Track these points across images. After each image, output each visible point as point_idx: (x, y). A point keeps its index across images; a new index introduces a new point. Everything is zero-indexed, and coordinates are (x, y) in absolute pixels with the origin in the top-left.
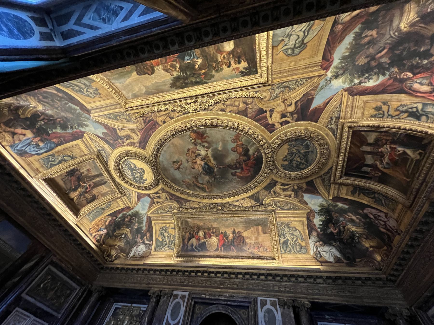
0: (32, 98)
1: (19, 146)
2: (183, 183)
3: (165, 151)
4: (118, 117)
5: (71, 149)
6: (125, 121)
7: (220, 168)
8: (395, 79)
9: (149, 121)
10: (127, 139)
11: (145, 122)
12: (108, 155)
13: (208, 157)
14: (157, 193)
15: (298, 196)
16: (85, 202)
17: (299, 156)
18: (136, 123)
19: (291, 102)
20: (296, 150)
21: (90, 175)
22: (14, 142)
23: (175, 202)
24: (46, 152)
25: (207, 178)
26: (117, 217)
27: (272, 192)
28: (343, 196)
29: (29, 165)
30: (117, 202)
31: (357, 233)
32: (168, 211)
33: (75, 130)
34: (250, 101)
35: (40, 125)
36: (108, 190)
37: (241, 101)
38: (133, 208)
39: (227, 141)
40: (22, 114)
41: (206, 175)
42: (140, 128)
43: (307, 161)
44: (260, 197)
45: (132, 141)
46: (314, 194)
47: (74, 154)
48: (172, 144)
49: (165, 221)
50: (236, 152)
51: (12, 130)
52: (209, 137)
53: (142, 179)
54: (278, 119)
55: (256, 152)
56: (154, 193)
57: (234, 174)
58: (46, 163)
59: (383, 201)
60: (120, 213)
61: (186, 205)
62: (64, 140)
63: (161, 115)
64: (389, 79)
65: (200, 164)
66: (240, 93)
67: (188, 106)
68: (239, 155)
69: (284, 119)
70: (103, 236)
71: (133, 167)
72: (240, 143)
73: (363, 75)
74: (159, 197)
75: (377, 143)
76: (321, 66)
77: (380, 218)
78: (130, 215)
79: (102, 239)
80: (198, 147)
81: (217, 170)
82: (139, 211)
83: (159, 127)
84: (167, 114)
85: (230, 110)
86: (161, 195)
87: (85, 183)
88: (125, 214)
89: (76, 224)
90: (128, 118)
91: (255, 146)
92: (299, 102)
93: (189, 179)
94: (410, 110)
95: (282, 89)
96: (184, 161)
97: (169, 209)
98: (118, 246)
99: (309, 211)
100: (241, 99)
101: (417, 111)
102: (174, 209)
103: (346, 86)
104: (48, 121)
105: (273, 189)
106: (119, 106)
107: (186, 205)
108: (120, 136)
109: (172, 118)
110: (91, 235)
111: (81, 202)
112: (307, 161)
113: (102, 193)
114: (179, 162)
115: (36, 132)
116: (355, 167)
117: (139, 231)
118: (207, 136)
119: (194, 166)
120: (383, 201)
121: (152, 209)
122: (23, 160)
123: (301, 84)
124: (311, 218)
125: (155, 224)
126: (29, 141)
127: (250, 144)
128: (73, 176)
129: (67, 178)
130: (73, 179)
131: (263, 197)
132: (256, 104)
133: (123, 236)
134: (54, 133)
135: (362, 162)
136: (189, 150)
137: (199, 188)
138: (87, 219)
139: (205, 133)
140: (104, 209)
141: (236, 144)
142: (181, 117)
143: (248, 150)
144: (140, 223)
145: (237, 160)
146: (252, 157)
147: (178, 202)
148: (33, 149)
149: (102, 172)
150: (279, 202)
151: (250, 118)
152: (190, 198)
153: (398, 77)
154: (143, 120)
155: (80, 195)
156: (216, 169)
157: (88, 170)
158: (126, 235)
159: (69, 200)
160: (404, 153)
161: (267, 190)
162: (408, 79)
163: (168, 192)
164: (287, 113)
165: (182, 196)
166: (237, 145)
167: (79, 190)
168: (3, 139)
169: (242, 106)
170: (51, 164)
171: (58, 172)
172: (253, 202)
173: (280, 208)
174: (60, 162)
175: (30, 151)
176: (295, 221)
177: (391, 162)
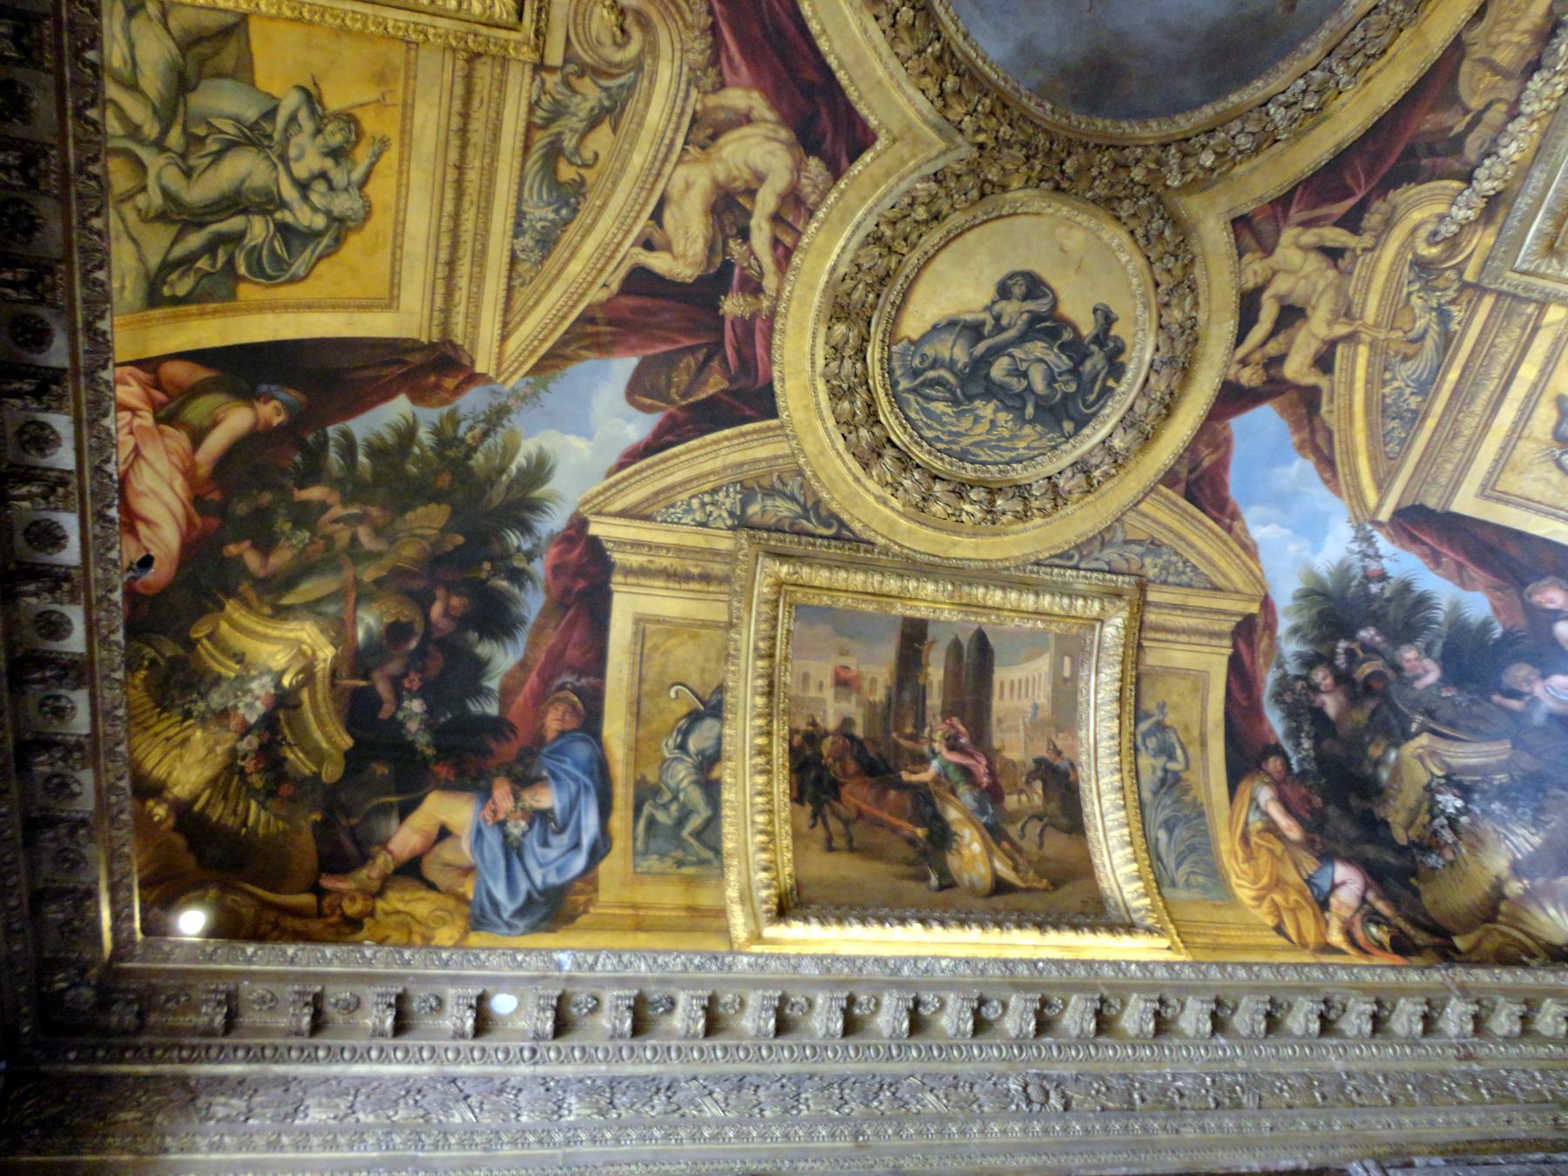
0: (231, 606)
1: (500, 893)
4: (566, 172)
5: (651, 672)
6: (604, 130)
10: (744, 234)
12: (793, 486)
16: (1057, 844)
18: (656, 58)
21: (880, 696)
22: (461, 899)
24: (605, 810)
26: (1277, 750)
30: (1167, 672)
32: (1443, 316)
33: (539, 568)
35: (428, 725)
36: (1043, 664)
38: (1267, 604)
40: (319, 764)
42: (699, 47)
45: (766, 201)
47: (694, 680)
49: (1518, 391)
51: (383, 861)
53: (1076, 350)
58: (679, 854)
60: (1255, 712)
61: (1475, 104)
62: (581, 673)
70: (1381, 906)
71: (961, 355)
74: (1291, 315)
78: (1309, 662)
79: (1403, 924)
82: (1312, 575)
86: (1281, 285)
87: (921, 761)
88: (1284, 684)
90: (591, 93)
97: (1428, 288)
102: (1453, 243)
104: (422, 671)
106: (483, 71)
107: (1475, 104)
108: (700, 280)
113: (1046, 711)
115: (461, 774)
117: (1473, 661)
121: (1351, 454)
122: (588, 928)
125: (1489, 491)
126: (493, 839)
128: (835, 788)
129: (835, 825)
130: (856, 795)
133: (1450, 802)
134: (506, 694)
140: (1169, 783)
144: (1407, 615)
147: (1408, 172)
148: (552, 853)
149: (899, 609)
155: (994, 833)
157: (844, 683)
158: (1454, 781)
163: (1282, 204)
165: (1389, 84)
167: (952, 814)
168: (416, 928)
170: (698, 834)
174: (711, 789)
175: (559, 870)
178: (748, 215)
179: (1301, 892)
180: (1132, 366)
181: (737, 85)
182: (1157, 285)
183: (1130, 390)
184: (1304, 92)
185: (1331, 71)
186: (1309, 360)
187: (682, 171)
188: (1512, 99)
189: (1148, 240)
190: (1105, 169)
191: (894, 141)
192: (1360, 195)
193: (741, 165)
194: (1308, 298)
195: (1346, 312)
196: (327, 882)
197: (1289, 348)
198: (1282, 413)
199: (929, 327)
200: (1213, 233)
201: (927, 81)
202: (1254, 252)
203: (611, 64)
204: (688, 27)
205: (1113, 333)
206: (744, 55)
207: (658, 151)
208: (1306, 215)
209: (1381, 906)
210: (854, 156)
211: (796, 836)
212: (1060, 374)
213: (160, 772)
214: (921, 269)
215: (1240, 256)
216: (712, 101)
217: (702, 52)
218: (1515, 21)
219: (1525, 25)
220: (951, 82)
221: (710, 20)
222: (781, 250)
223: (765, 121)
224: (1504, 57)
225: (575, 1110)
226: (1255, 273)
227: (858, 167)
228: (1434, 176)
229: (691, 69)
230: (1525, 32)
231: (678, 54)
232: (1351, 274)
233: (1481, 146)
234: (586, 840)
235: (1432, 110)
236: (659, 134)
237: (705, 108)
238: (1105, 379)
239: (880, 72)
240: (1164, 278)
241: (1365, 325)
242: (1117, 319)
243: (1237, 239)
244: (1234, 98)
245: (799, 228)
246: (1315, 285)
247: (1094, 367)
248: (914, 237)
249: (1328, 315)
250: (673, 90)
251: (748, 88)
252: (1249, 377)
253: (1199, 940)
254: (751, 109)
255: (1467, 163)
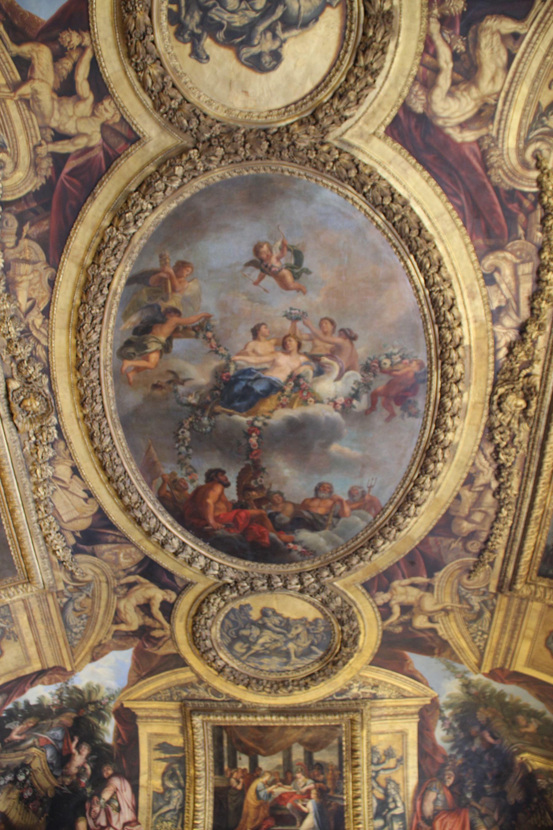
2: (173, 264)
3: (360, 231)
7: (248, 435)
8: (444, 766)
9: (511, 218)
10: (455, 56)
11: (513, 195)
13: (305, 402)
14: (100, 89)
15: (121, 639)
17: (276, 641)
18: (518, 148)
19: (437, 622)
20: (298, 635)
23: (37, 182)
25: (199, 375)
27: (132, 579)
28: (145, 731)
31: (27, 777)
34: (475, 546)
37: (479, 528)
39: (361, 475)
41: (218, 374)
43: (257, 655)
44: (104, 547)
45: (444, 81)
46: (132, 670)
48: (391, 279)
50: (312, 495)
52: (388, 420)
53: (211, 27)
54: (401, 598)
55: (305, 548)
56: (95, 64)
57: (215, 477)
59: (166, 809)
61: (24, 242)
63: (522, 279)
64: (445, 757)
65: (274, 363)
66: (506, 532)
67: (519, 386)
68: (298, 501)
69: (397, 610)
72: (347, 509)
73: (456, 720)
74: (66, 89)
75: (312, 767)
76: (502, 669)
77: (113, 813)
80: (354, 376)
81: (238, 424)
83: (476, 249)
84: (517, 302)
85: (463, 498)
91: (328, 548)
92: (431, 635)
93: (198, 297)
94: (390, 800)
95: (477, 608)
96: (300, 302)
99: (69, 668)
100: (487, 528)
101: (390, 810)
103: (442, 700)
105: (142, 580)
107: (24, 242)
109: (496, 316)
112: (257, 655)
114: (296, 277)
116: (243, 739)
118: (392, 415)
119: (267, 338)
120: (166, 809)
123: (474, 638)
124: (46, 679)
127: (336, 537)
131: (106, 555)
132: (458, 557)
135: (262, 751)
136: (352, 337)
137: (144, 330)
139: (405, 409)
141: (345, 498)
142: (492, 350)
143: (314, 525)
145: (281, 494)
146: (285, 537)
150: (92, 597)
151: (424, 542)
152: (70, 273)
153: (447, 768)
154: (525, 194)
156: (242, 419)
160: (304, 815)
161: (140, 564)
162: (443, 781)
164: (413, 614)
166: (341, 501)
169: (466, 526)
172: (84, 524)
173: (66, 604)
176: (25, 649)
177: (275, 800)
178: (454, 69)
180: (165, 24)
181: (470, 143)
182: (174, 86)
183: (159, 6)
184: (135, 221)
185: (125, 235)
186: (36, 62)
187: (498, 88)
188: (6, 251)
189: (195, 114)
190: (241, 149)
191: (374, 134)
192: (63, 176)
193: (463, 100)
194: (61, 105)
195: (29, 103)
197: (54, 67)
198: (32, 18)
199: (321, 19)
200: (148, 126)
201: (367, 171)
202: (115, 124)
203: (542, 140)
204: (500, 167)
205: (189, 45)
206: (468, 160)
207: (513, 97)
208: (92, 154)
210: (396, 119)
212: (214, 5)
214: (338, 58)
215: (122, 118)
216: (484, 132)
217: (491, 156)
218: (30, 285)
219: (25, 285)
220: (353, 173)
221: (489, 173)
222: (431, 51)
223: (452, 127)
224: (24, 268)
226: (106, 110)
227: (393, 114)
228: (24, 198)
229: (496, 146)
230: (21, 282)
231: (505, 152)
232: (40, 128)
233: (7, 223)
235: (48, 232)
236: (513, 106)
237: (487, 126)
238: (179, 8)
239: (391, 168)
240: (173, 93)
241: (11, 98)
242: (190, 55)
243: (131, 128)
244: (174, 205)
245: (422, 68)
246: (61, 114)
247: (192, 17)
248: (352, 81)
249: (40, 97)
250: (507, 132)
251: (463, 143)
252: (73, 39)
254: (461, 132)
255: (9, 212)
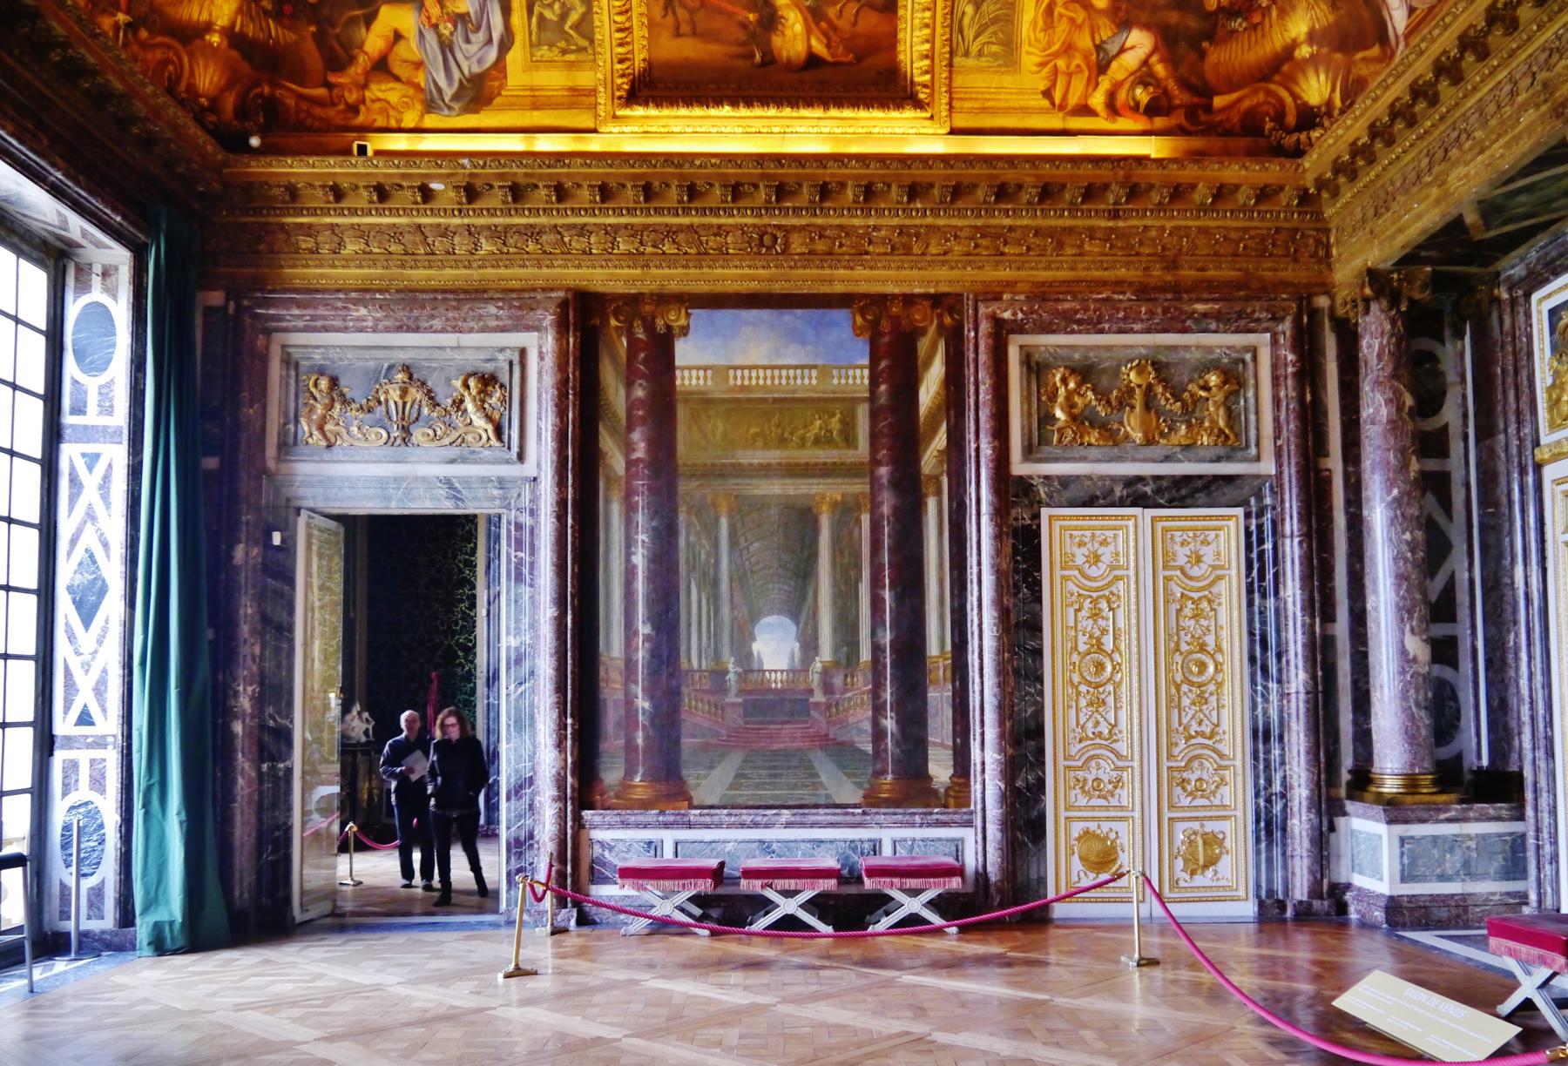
22: (417, 87)
29: (536, 105)
58: (562, 44)
70: (1160, 70)
89: (953, 132)
98: (1312, 37)
110: (1085, 110)
111: (853, 36)
129: (682, 14)
138: (980, 70)
148: (473, 48)
159: (807, 76)
168: (392, 113)
170: (577, 27)
171: (628, 30)
175: (479, 61)
179: (1086, 58)
196: (333, 79)
209: (1160, 70)
211: (652, 25)
213: (205, 17)
225: (486, 246)
234: (496, 37)
253: (968, 105)
